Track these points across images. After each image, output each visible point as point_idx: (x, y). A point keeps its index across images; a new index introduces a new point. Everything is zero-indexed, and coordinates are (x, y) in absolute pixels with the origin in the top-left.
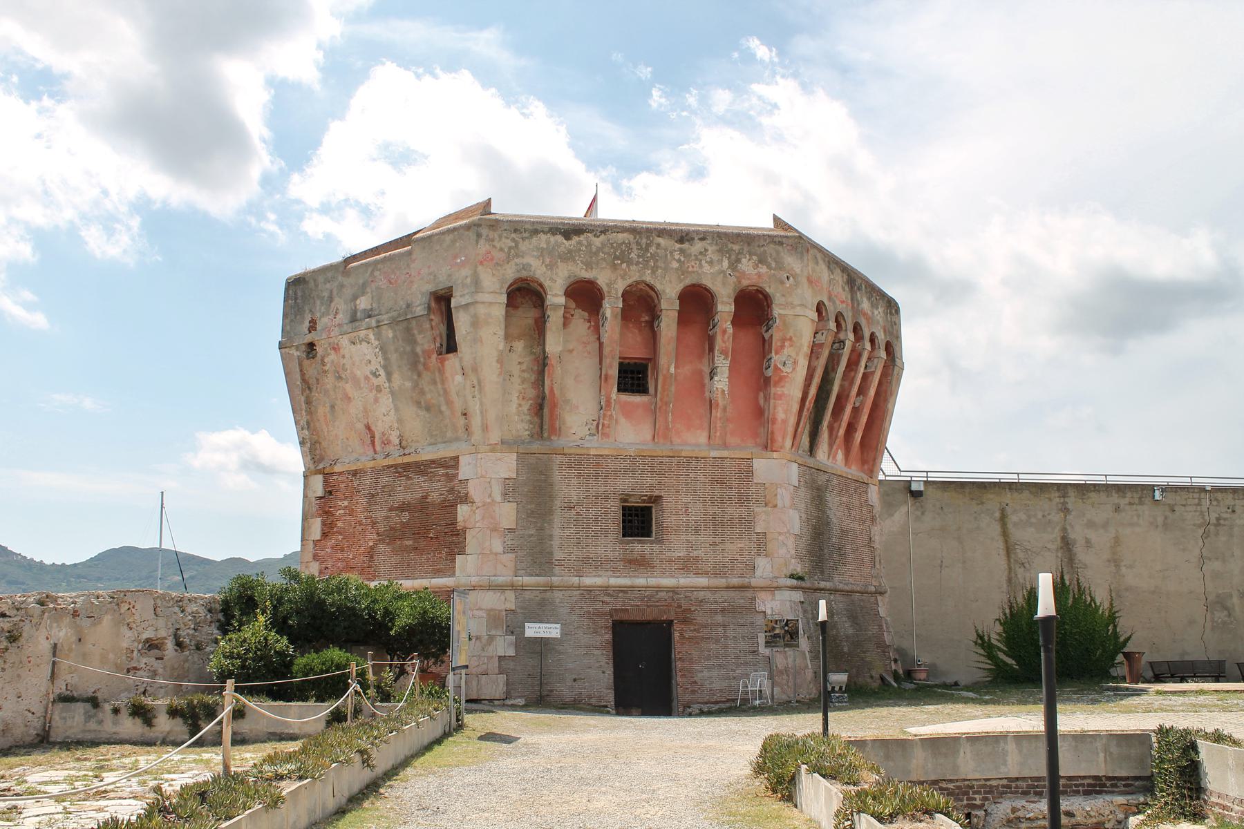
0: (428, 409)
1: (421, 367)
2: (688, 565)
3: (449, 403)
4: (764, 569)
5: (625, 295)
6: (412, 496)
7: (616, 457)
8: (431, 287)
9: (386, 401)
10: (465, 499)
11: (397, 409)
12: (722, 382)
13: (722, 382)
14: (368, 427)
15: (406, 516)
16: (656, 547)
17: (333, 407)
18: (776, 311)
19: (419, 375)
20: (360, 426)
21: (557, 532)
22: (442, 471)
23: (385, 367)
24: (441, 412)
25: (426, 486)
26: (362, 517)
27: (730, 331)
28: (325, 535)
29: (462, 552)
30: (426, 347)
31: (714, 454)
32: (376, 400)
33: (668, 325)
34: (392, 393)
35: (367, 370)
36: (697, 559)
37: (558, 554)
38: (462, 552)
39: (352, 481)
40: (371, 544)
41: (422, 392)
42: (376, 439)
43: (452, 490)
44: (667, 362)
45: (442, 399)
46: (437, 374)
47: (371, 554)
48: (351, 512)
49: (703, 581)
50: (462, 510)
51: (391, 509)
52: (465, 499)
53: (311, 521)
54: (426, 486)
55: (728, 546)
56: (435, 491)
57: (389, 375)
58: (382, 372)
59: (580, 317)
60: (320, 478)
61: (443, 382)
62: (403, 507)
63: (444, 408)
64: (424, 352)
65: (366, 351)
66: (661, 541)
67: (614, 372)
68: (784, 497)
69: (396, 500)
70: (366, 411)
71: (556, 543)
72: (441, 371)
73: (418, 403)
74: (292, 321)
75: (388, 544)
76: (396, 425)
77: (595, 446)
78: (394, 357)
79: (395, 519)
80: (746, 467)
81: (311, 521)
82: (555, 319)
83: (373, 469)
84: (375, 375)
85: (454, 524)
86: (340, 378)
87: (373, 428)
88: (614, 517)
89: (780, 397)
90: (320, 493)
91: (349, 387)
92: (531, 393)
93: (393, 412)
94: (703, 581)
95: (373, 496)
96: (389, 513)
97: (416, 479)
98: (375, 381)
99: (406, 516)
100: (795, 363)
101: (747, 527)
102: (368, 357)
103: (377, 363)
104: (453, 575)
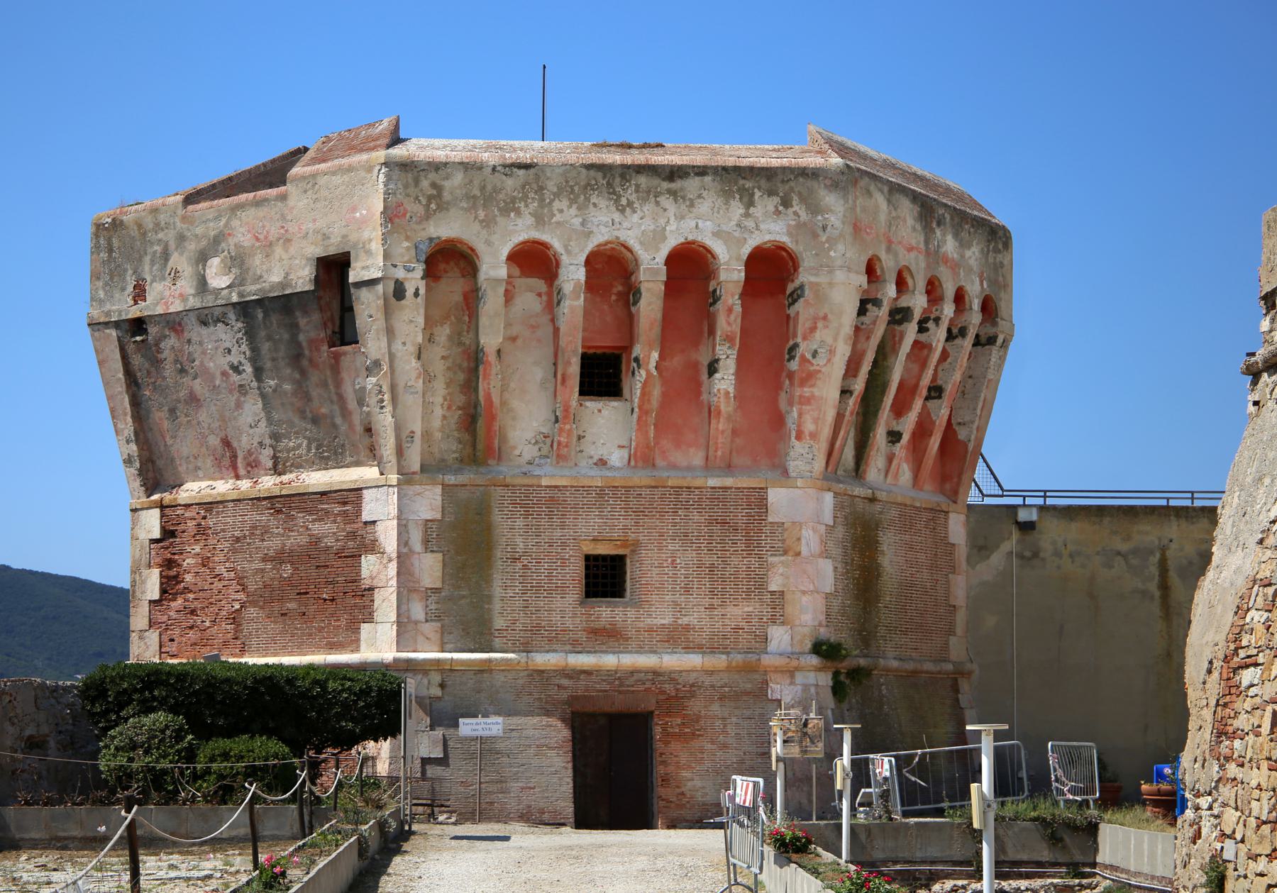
0: (315, 421)
1: (305, 363)
2: (676, 637)
3: (346, 413)
4: (779, 637)
5: (588, 262)
6: (296, 540)
7: (576, 488)
8: (320, 252)
9: (253, 408)
11: (270, 420)
12: (725, 382)
13: (725, 382)
14: (226, 443)
16: (631, 613)
17: (172, 411)
18: (804, 277)
19: (303, 373)
20: (214, 441)
21: (497, 591)
24: (334, 426)
25: (317, 528)
26: (221, 569)
27: (738, 309)
28: (163, 591)
29: (369, 619)
30: (313, 334)
31: (712, 482)
32: (239, 405)
33: (650, 306)
34: (263, 396)
35: (223, 362)
36: (687, 628)
37: (499, 623)
38: (369, 619)
39: (204, 518)
40: (237, 606)
41: (307, 398)
42: (239, 460)
43: (352, 535)
44: (647, 354)
45: (336, 407)
46: (328, 373)
47: (235, 619)
48: (205, 562)
49: (694, 660)
51: (264, 560)
52: (372, 547)
53: (145, 572)
54: (317, 528)
55: (732, 610)
56: (328, 531)
57: (258, 373)
58: (248, 369)
59: (529, 298)
60: (156, 513)
61: (338, 383)
62: (280, 557)
63: (338, 421)
64: (311, 342)
65: (223, 337)
66: (638, 605)
67: (575, 369)
68: (810, 541)
69: (273, 544)
71: (497, 606)
72: (336, 368)
73: (302, 413)
74: (106, 284)
75: (262, 608)
76: (268, 441)
77: (551, 476)
80: (759, 502)
81: (145, 572)
82: (492, 303)
84: (236, 369)
85: (356, 580)
86: (182, 371)
87: (235, 444)
88: (576, 570)
89: (807, 401)
90: (156, 534)
91: (198, 386)
92: (460, 399)
93: (263, 424)
94: (694, 660)
95: (238, 540)
96: (261, 565)
97: (301, 518)
98: (235, 378)
99: (287, 570)
100: (832, 352)
101: (757, 584)
102: (228, 345)
103: (241, 353)
104: (354, 645)
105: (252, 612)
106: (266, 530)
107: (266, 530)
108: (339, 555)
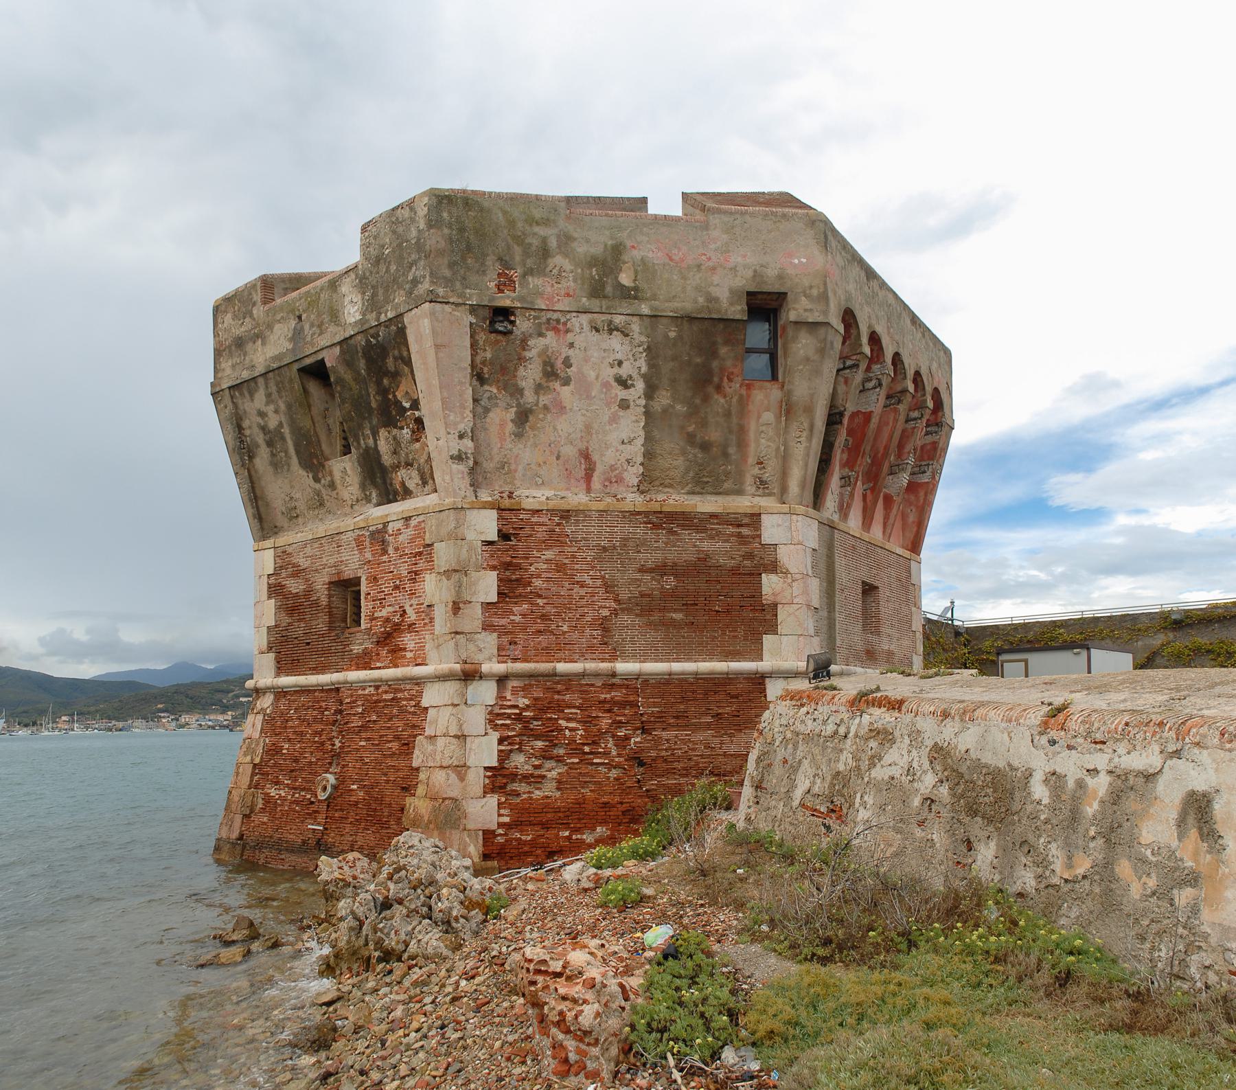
9: (631, 426)
10: (774, 567)
15: (670, 582)
22: (731, 529)
23: (646, 378)
32: (614, 419)
34: (647, 414)
47: (604, 626)
50: (770, 584)
51: (642, 570)
52: (774, 567)
54: (706, 545)
56: (721, 550)
60: (493, 514)
62: (661, 570)
69: (651, 558)
70: (588, 428)
78: (666, 367)
79: (649, 583)
83: (602, 513)
96: (638, 576)
99: (670, 582)
105: (626, 619)
106: (641, 545)
107: (641, 545)
108: (735, 571)
